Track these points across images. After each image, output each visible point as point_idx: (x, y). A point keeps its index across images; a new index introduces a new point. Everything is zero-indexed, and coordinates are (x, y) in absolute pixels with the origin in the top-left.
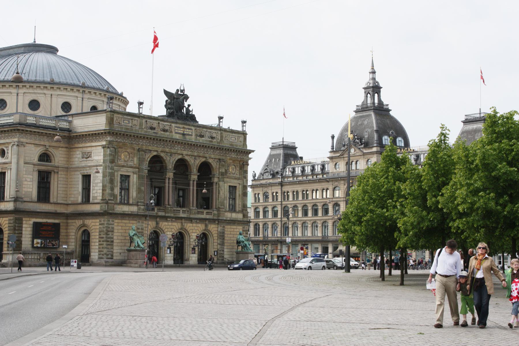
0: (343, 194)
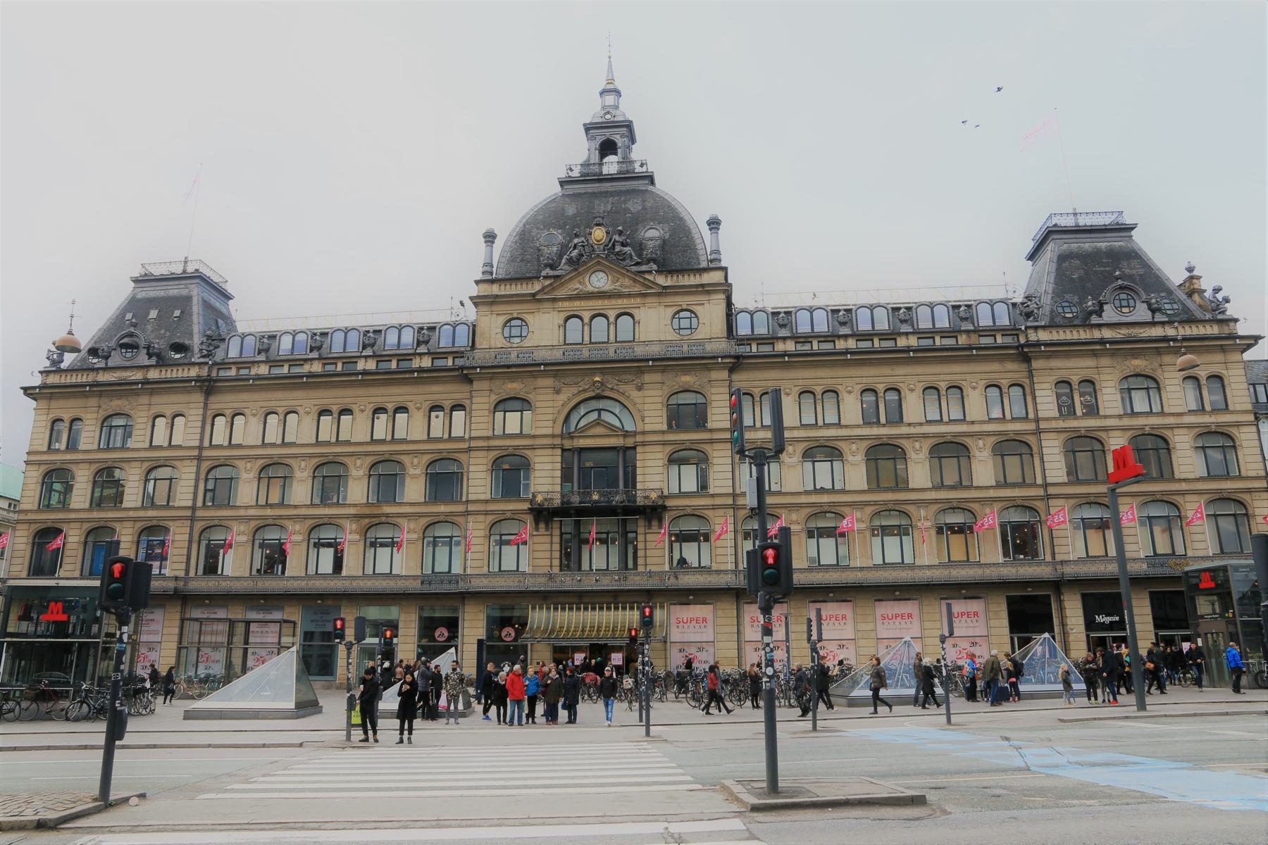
0: (550, 424)
